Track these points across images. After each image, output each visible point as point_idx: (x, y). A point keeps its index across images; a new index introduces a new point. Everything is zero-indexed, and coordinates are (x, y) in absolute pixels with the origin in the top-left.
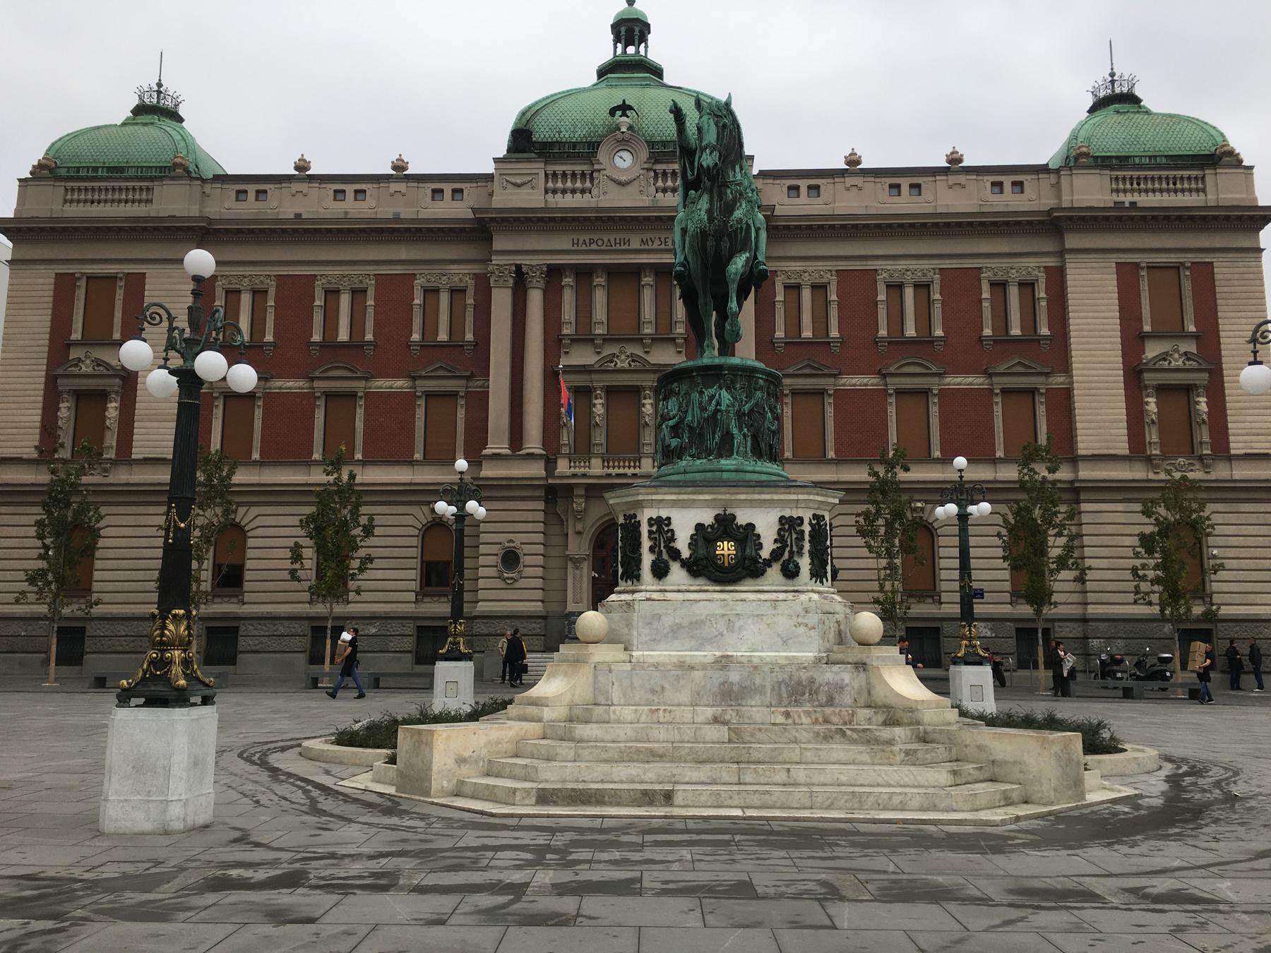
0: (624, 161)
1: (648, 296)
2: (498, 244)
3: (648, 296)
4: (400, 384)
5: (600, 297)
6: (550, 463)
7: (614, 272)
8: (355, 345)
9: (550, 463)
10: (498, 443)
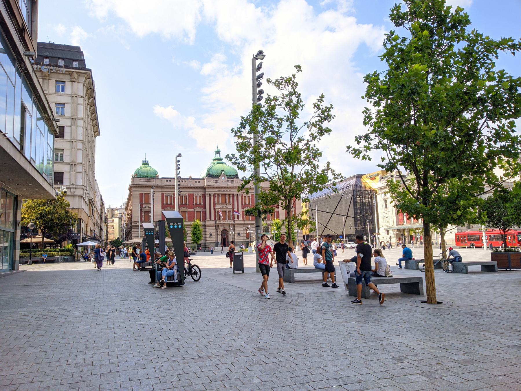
0: (223, 178)
1: (227, 198)
2: (207, 190)
3: (227, 198)
4: (193, 210)
5: (220, 198)
6: (216, 222)
7: (222, 194)
8: (186, 204)
9: (216, 222)
10: (208, 219)
